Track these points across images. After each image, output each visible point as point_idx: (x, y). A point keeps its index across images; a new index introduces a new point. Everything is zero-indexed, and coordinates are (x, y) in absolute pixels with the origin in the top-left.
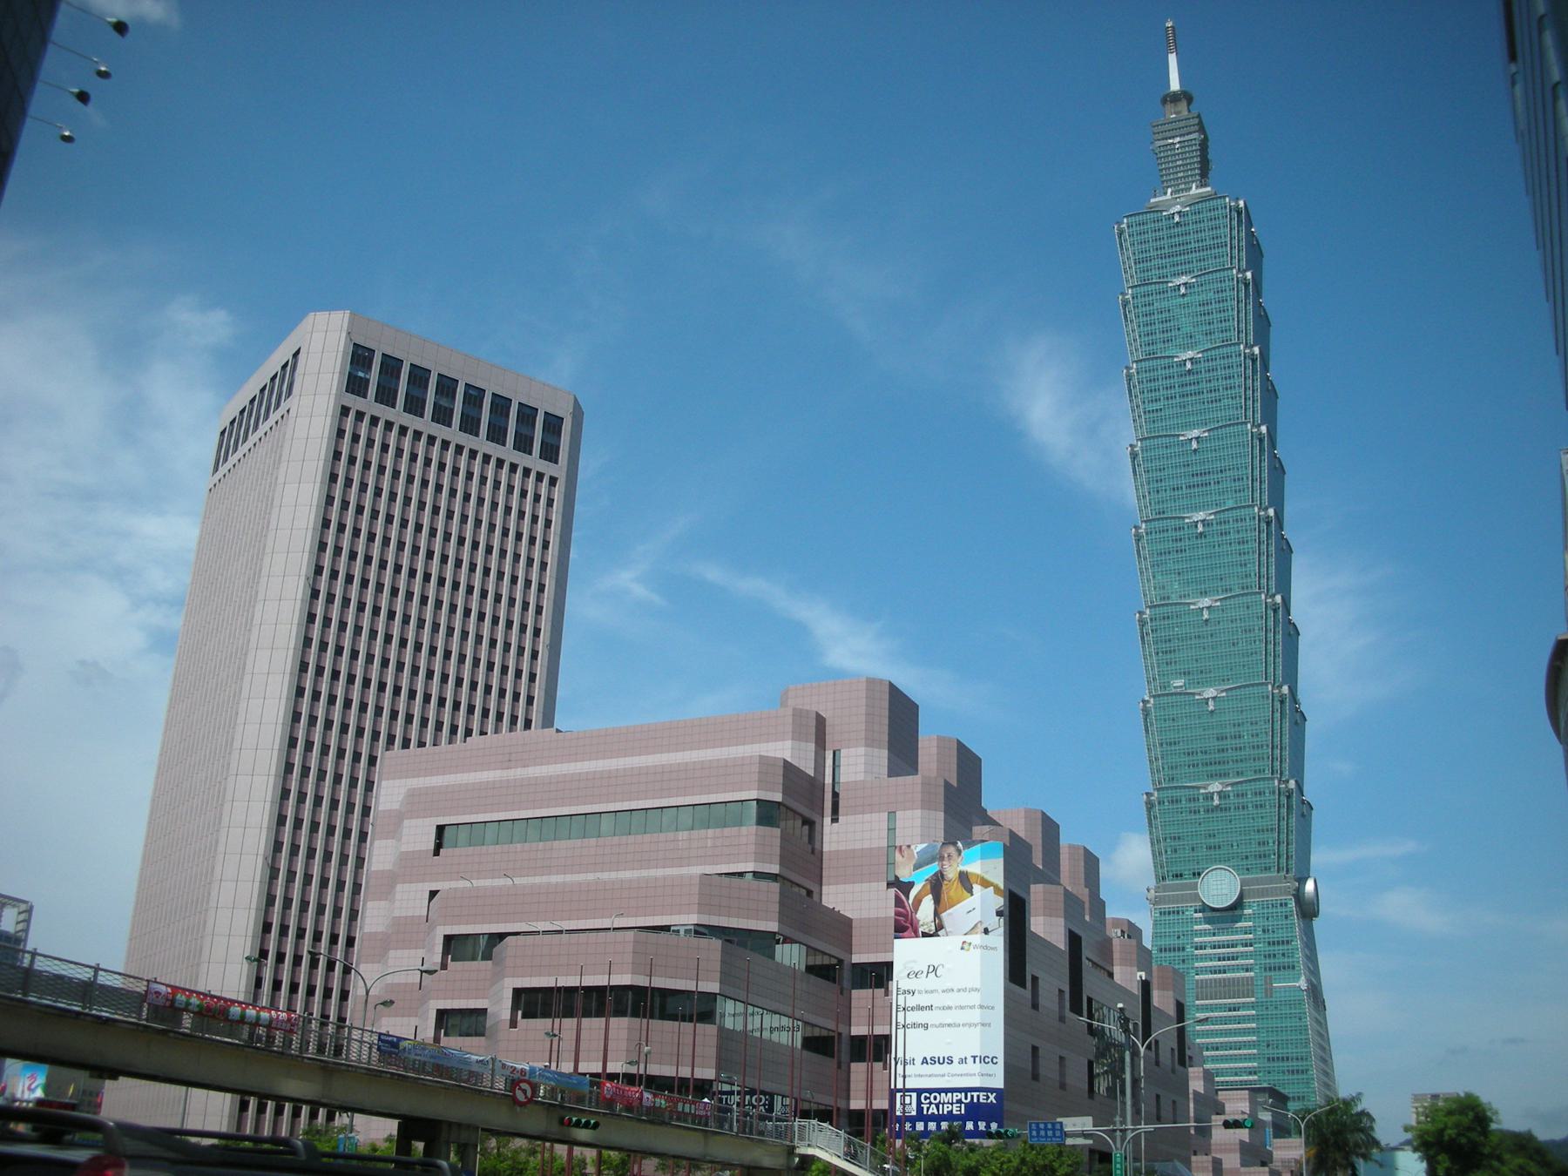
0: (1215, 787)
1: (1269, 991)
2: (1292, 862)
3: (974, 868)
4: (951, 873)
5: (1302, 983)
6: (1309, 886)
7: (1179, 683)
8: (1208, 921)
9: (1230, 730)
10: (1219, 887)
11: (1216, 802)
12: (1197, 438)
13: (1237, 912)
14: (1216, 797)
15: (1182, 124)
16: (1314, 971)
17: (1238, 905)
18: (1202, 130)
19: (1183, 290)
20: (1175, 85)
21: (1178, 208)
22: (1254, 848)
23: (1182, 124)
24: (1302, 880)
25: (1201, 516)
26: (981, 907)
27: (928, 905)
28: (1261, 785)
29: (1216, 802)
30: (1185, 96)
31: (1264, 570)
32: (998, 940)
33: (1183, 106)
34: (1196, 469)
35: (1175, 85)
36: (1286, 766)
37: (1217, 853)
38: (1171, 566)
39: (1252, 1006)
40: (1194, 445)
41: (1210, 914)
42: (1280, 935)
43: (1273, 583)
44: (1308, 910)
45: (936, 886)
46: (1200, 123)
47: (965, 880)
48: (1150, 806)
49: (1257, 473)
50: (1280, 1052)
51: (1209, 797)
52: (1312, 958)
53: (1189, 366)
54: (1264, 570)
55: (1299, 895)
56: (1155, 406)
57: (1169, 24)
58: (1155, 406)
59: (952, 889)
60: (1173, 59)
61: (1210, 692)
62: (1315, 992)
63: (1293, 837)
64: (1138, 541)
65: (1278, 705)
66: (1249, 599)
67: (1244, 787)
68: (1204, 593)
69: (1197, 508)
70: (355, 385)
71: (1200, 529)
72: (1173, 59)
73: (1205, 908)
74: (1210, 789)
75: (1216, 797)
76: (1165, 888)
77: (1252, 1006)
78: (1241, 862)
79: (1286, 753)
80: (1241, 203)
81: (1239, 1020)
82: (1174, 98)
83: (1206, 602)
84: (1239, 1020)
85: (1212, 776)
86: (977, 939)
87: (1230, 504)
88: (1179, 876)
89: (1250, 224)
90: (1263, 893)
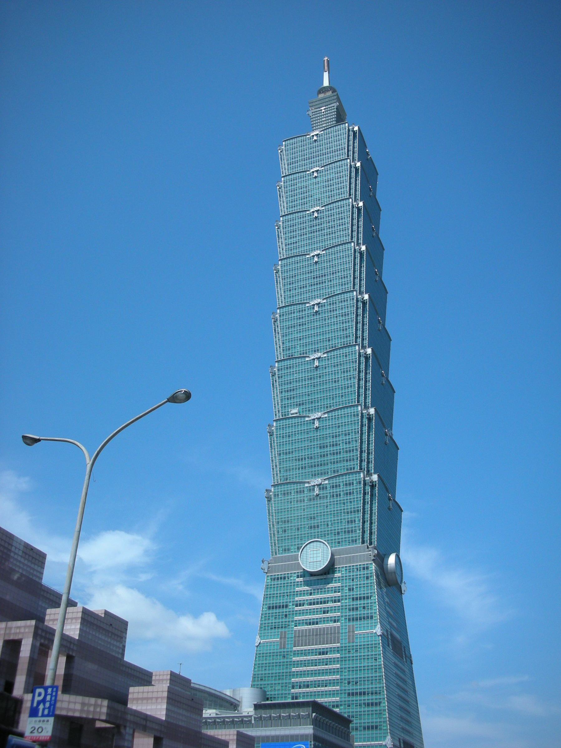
2: (375, 537)
6: (392, 560)
8: (307, 583)
9: (329, 440)
10: (315, 557)
13: (329, 576)
14: (316, 489)
15: (327, 100)
17: (329, 570)
18: (338, 100)
19: (315, 174)
20: (326, 83)
22: (345, 526)
23: (327, 100)
30: (330, 88)
31: (360, 333)
33: (330, 93)
35: (326, 83)
36: (372, 465)
37: (315, 531)
39: (338, 650)
40: (316, 259)
41: (308, 578)
43: (366, 342)
48: (269, 499)
49: (358, 274)
50: (358, 688)
51: (311, 489)
54: (360, 333)
56: (292, 240)
57: (326, 59)
58: (292, 240)
60: (326, 75)
63: (375, 518)
65: (366, 421)
67: (337, 480)
69: (315, 298)
72: (326, 75)
73: (305, 574)
74: (312, 484)
75: (316, 489)
76: (276, 560)
77: (338, 650)
78: (335, 537)
79: (372, 457)
80: (356, 128)
81: (327, 662)
82: (324, 90)
84: (327, 662)
85: (315, 475)
89: (363, 145)
90: (350, 560)
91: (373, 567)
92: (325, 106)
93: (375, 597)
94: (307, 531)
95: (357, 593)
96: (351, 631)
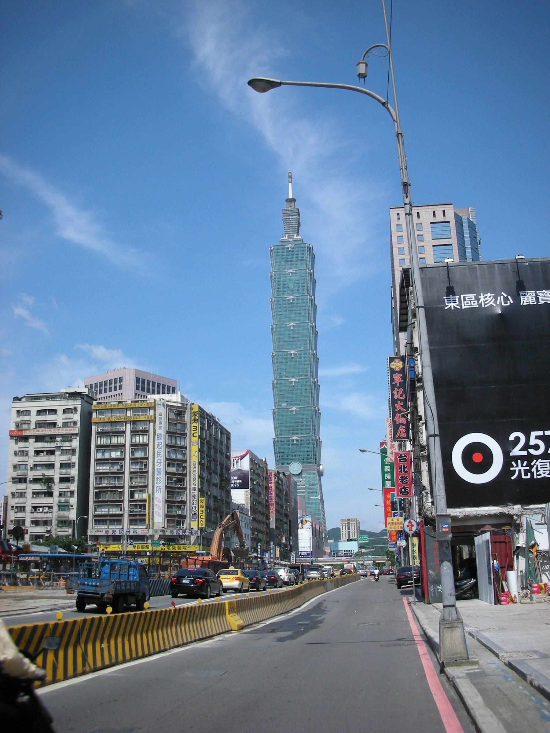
0: (295, 438)
1: (309, 499)
3: (307, 519)
4: (304, 520)
5: (319, 497)
6: (321, 467)
7: (285, 404)
9: (299, 420)
11: (295, 442)
12: (293, 326)
15: (293, 212)
16: (321, 493)
18: (299, 215)
21: (290, 245)
22: (306, 457)
23: (293, 212)
24: (319, 465)
25: (293, 352)
26: (308, 524)
27: (300, 524)
28: (307, 438)
29: (295, 442)
32: (311, 530)
33: (293, 204)
34: (293, 336)
38: (283, 367)
42: (313, 483)
44: (321, 474)
45: (302, 521)
46: (299, 212)
47: (306, 521)
52: (321, 489)
53: (291, 301)
55: (318, 471)
59: (304, 522)
60: (290, 184)
61: (294, 408)
62: (322, 499)
64: (273, 358)
65: (314, 413)
66: (306, 380)
68: (293, 376)
70: (137, 388)
71: (293, 356)
72: (290, 184)
83: (293, 380)
85: (293, 434)
86: (308, 530)
87: (302, 348)
88: (283, 464)
90: (308, 470)
91: (317, 474)
92: (292, 216)
93: (318, 485)
94: (291, 457)
95: (311, 483)
96: (309, 496)
